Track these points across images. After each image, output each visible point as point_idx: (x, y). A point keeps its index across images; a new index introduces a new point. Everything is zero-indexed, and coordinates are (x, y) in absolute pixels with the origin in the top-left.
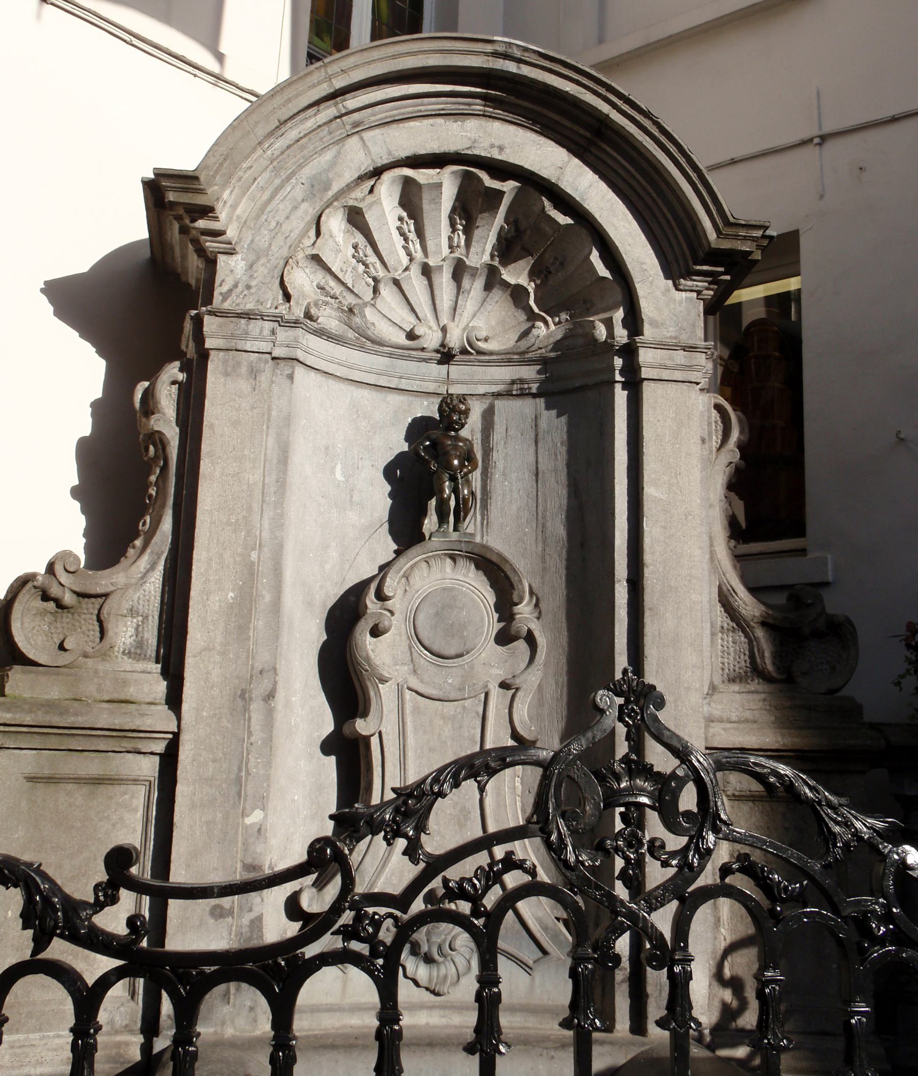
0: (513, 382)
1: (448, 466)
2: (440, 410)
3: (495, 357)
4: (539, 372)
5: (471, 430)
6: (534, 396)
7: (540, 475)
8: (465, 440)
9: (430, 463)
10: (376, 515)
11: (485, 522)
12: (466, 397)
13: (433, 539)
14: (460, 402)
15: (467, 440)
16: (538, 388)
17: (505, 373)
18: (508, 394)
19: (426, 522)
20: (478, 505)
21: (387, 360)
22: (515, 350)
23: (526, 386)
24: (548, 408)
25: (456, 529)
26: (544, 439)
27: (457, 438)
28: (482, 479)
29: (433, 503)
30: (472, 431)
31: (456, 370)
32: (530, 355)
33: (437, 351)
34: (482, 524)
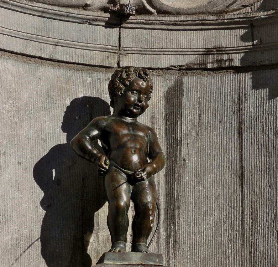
0: (208, 52)
1: (125, 164)
2: (112, 89)
3: (183, 18)
4: (243, 38)
5: (153, 116)
6: (237, 70)
7: (246, 177)
8: (146, 129)
9: (100, 158)
10: (24, 231)
11: (172, 240)
12: (148, 71)
13: (106, 262)
14: (140, 76)
15: (149, 128)
16: (242, 60)
17: (199, 40)
18: (201, 68)
19: (92, 240)
20: (162, 217)
21: (37, 21)
22: (210, 9)
23: (225, 57)
24: (256, 86)
25: (135, 248)
26: (250, 128)
27: (135, 126)
28: (167, 183)
29: (102, 214)
30: (152, 117)
31: (129, 36)
32: (231, 15)
33: (105, 9)
34: (168, 243)
